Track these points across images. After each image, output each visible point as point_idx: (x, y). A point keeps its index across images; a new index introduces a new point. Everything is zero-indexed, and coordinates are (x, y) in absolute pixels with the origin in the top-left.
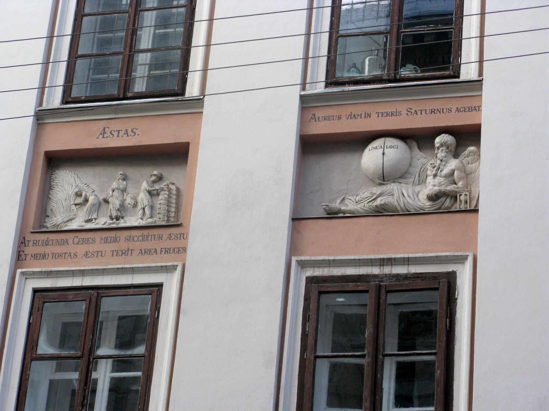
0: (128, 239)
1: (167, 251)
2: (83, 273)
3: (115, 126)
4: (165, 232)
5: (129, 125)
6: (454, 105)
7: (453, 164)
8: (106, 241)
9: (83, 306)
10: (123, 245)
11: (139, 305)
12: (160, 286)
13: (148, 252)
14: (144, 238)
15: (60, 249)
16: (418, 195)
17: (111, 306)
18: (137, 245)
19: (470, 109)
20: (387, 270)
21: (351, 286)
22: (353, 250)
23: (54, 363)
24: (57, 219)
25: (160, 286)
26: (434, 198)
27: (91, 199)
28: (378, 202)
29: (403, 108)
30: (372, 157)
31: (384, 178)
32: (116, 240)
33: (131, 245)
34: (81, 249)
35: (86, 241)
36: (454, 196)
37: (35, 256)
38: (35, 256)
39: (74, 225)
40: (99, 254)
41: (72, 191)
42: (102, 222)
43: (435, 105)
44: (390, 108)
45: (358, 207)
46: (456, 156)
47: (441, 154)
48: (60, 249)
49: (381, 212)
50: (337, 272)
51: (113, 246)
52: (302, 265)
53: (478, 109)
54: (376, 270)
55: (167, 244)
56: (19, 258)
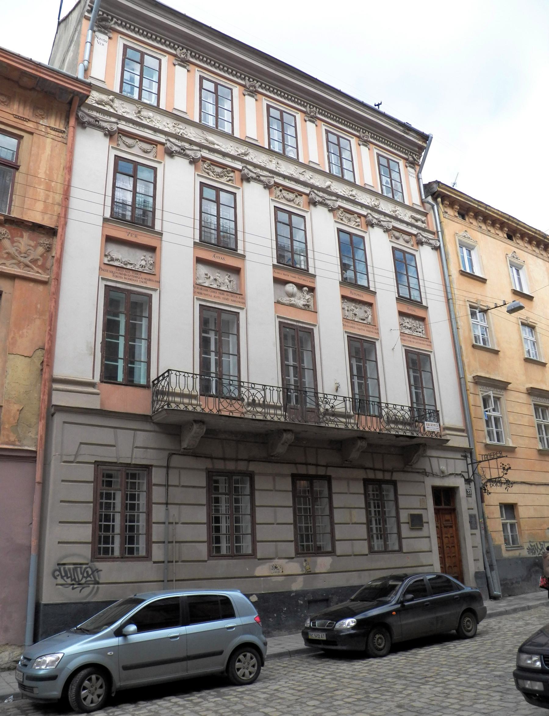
0: (227, 295)
1: (240, 302)
2: (215, 303)
3: (217, 255)
4: (238, 296)
5: (223, 256)
6: (309, 280)
7: (308, 297)
8: (220, 293)
10: (226, 297)
12: (239, 313)
13: (234, 301)
14: (232, 296)
15: (206, 292)
16: (301, 303)
18: (231, 298)
19: (313, 282)
20: (298, 324)
21: (291, 327)
22: (293, 315)
24: (200, 281)
26: (304, 305)
27: (212, 278)
28: (292, 302)
29: (297, 276)
30: (291, 288)
31: (292, 295)
32: (223, 294)
33: (228, 297)
34: (213, 294)
35: (214, 292)
36: (308, 306)
37: (198, 293)
38: (198, 293)
39: (206, 285)
40: (219, 297)
41: (204, 273)
42: (215, 286)
43: (304, 278)
44: (294, 275)
45: (286, 302)
46: (307, 294)
47: (305, 293)
48: (206, 292)
49: (292, 305)
50: (289, 322)
52: (278, 317)
53: (314, 283)
54: (295, 323)
55: (239, 300)
56: (194, 292)
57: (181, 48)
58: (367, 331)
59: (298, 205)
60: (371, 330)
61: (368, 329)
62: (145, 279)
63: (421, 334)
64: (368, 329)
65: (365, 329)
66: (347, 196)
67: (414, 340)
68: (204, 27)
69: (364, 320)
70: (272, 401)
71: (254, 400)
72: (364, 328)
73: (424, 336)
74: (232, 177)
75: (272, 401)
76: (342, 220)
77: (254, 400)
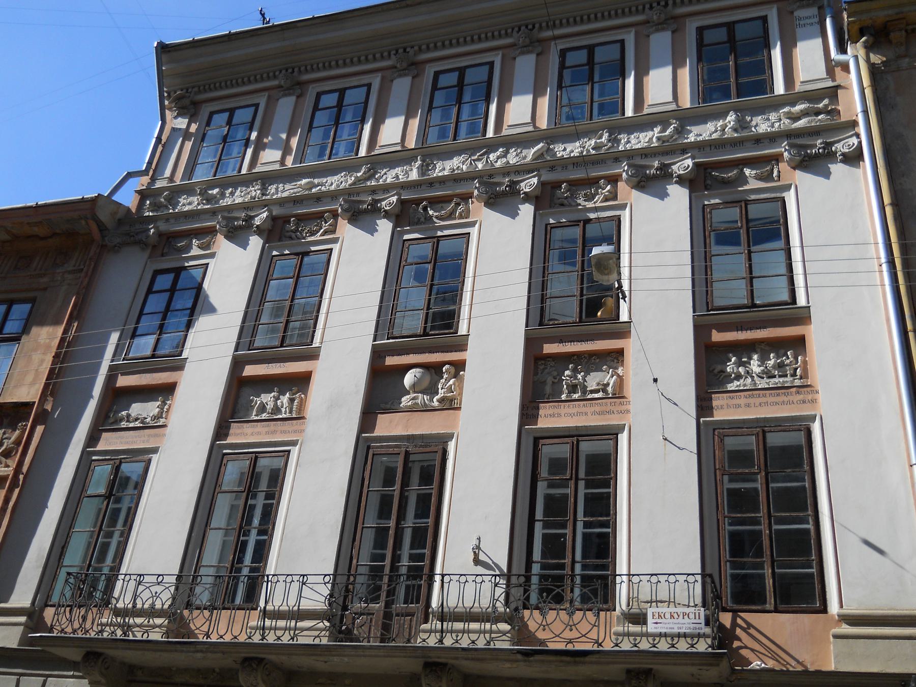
1: (295, 432)
9: (248, 462)
11: (278, 463)
12: (289, 451)
13: (284, 432)
17: (263, 462)
23: (234, 494)
25: (289, 451)
26: (441, 401)
36: (451, 400)
40: (259, 433)
42: (264, 416)
51: (267, 429)
55: (295, 428)
57: (284, 72)
58: (594, 413)
59: (461, 217)
60: (609, 408)
61: (597, 409)
62: (149, 436)
63: (789, 379)
64: (597, 409)
65: (590, 410)
66: (584, 153)
67: (751, 401)
68: (299, 25)
69: (597, 391)
70: (285, 603)
71: (153, 605)
72: (584, 410)
73: (797, 382)
74: (330, 225)
75: (285, 603)
76: (562, 205)
77: (153, 605)
